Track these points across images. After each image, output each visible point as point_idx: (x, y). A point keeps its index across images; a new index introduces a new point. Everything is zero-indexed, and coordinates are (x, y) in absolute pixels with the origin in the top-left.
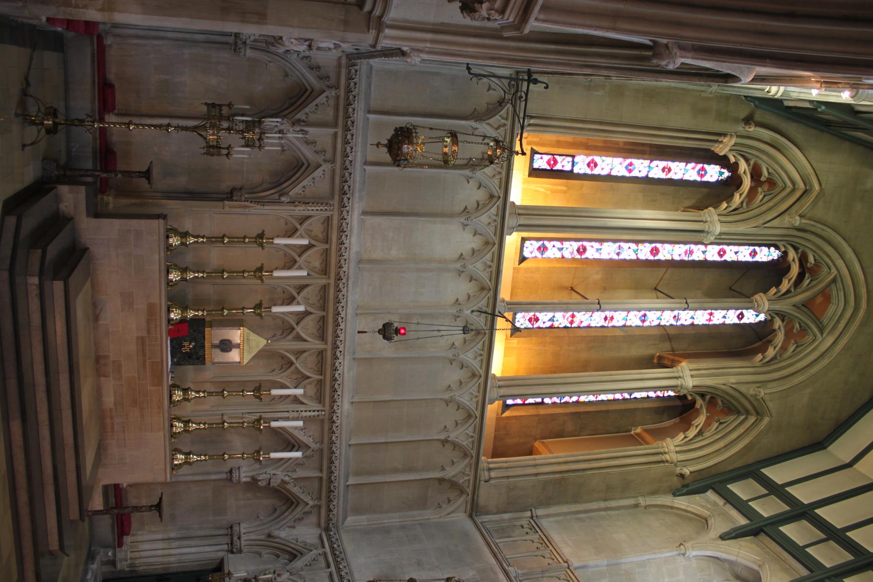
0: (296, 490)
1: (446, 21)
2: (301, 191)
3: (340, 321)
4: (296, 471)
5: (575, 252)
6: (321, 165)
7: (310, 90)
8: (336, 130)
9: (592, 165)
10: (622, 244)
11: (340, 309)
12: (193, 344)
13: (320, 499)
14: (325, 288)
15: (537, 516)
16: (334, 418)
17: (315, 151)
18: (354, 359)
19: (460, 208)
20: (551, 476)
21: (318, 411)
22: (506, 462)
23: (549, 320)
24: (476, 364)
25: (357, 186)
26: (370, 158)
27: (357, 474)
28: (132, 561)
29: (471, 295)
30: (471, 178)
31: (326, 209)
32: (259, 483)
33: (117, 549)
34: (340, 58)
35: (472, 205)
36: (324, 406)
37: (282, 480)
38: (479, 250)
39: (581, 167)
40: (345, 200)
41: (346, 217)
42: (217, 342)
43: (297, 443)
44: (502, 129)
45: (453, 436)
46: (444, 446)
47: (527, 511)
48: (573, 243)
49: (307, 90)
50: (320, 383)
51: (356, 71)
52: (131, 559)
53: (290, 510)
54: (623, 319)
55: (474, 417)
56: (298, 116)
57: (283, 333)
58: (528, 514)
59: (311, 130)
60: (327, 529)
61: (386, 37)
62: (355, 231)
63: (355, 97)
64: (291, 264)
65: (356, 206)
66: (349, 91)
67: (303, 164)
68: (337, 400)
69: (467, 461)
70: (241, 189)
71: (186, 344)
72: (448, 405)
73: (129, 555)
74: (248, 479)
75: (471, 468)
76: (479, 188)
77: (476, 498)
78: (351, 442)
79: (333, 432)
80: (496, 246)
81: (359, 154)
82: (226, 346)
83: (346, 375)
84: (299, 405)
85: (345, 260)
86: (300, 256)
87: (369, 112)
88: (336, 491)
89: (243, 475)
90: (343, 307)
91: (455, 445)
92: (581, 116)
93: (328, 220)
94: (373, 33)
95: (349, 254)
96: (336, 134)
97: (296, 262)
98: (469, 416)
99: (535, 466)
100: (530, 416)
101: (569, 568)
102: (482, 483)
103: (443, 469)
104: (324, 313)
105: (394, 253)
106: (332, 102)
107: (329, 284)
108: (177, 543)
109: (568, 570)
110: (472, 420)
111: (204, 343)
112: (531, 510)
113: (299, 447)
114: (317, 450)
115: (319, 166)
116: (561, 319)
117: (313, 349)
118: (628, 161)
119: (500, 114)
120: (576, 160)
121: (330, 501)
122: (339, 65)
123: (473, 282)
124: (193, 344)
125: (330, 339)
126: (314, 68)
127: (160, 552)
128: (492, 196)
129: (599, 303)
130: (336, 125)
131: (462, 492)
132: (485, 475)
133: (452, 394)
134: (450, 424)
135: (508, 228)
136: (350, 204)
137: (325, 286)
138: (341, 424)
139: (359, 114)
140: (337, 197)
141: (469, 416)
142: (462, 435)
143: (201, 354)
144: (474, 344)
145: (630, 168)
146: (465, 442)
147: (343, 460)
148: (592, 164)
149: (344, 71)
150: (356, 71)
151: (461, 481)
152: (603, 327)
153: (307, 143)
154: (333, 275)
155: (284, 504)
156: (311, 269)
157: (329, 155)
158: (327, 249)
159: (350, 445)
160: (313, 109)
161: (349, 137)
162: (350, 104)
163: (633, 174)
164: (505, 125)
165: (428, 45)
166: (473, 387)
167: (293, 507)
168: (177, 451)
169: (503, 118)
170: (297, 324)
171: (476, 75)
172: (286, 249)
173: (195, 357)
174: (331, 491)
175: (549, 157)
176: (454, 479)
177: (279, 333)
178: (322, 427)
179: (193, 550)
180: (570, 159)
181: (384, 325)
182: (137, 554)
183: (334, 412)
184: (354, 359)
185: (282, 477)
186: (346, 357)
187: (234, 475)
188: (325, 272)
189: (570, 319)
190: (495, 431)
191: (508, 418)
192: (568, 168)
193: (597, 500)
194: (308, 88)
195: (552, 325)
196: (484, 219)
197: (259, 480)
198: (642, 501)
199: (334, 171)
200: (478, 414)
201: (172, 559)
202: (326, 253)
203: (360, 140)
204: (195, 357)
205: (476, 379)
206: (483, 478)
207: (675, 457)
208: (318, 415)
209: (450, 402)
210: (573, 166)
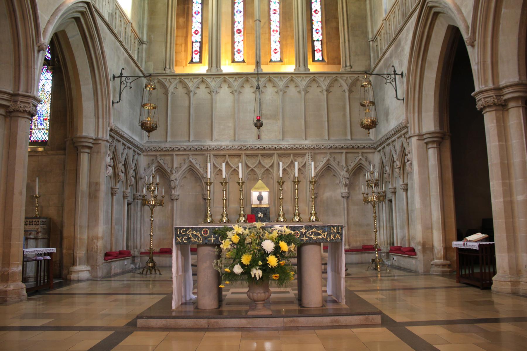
0: (353, 165)
1: (93, 114)
2: (202, 169)
3: (262, 147)
4: (342, 165)
5: (240, 34)
6: (190, 161)
7: (158, 167)
8: (174, 155)
9: (196, 32)
10: (235, 11)
11: (256, 148)
12: (259, 212)
13: (358, 153)
14: (247, 155)
15: (372, 38)
16: (312, 147)
17: (184, 163)
18: (283, 140)
19: (209, 96)
20: (350, 33)
21: (309, 156)
22: (343, 58)
23: (276, 43)
25: (199, 144)
26: (187, 139)
27: (346, 135)
28: (388, 244)
29: (250, 86)
30: (194, 92)
31: (210, 157)
32: (347, 183)
33: (381, 251)
34: (144, 155)
35: (207, 90)
36: (307, 153)
37: (346, 172)
38: (229, 85)
39: (198, 38)
40: (204, 149)
41: (212, 148)
42: (258, 202)
43: (327, 165)
44: (171, 80)
45: (325, 88)
46: (331, 92)
47: (369, 44)
48: (235, 37)
49: (158, 169)
50: (295, 155)
51: (148, 148)
52: (387, 245)
53: (365, 168)
54: (275, 4)
55: (314, 78)
56: (169, 171)
57: (270, 174)
58: (371, 43)
59: (175, 165)
60: (375, 148)
61: (103, 137)
62: (219, 143)
63: (159, 148)
64: (236, 171)
65: (209, 143)
66: (157, 151)
67: (190, 168)
68: (303, 147)
69: (340, 79)
70: (203, 195)
71: (259, 215)
72: (308, 92)
73: (386, 246)
74: (346, 188)
75: (343, 77)
76: (199, 88)
77: (359, 72)
78: (327, 138)
79: (320, 148)
80: (225, 77)
81: (184, 144)
82: (260, 198)
83: (290, 143)
84: (307, 165)
85: (233, 147)
86: (232, 168)
87: (189, 141)
88: (353, 145)
89: (344, 191)
90: (255, 146)
91: (330, 86)
92: (164, 44)
93: (215, 156)
94: (100, 142)
95: (230, 145)
96: (176, 155)
97: (235, 170)
99: (345, 42)
100: (327, 47)
101: (385, 19)
102: (352, 70)
103: (344, 91)
104: (260, 155)
105: (231, 125)
106: (163, 158)
107: (245, 154)
108: (381, 223)
109: (386, 19)
110: (316, 79)
111: (259, 208)
112: (369, 42)
113: (329, 164)
114: (331, 155)
115: (190, 161)
116: (275, 37)
117: (277, 160)
118: (194, 14)
119: (164, 82)
120: (194, 41)
121: (358, 147)
122: (147, 155)
123: (244, 86)
124: (259, 212)
125: (272, 152)
126: (149, 166)
127: (385, 231)
128: (203, 81)
129: (256, 21)
130: (172, 155)
131: (357, 80)
132: (348, 68)
133: (302, 90)
134: (319, 90)
135: (218, 72)
136: (207, 146)
137: (246, 155)
138: (316, 144)
139: (167, 145)
140: (204, 153)
141: (314, 80)
142: (324, 83)
143: (264, 209)
144: (275, 82)
145: (197, 13)
146: (327, 82)
147: (336, 142)
148: (196, 32)
149: (149, 153)
150: (148, 148)
151: (350, 81)
152: (279, 14)
153: (180, 167)
154: (240, 152)
155: (363, 171)
156: (239, 162)
157: (186, 157)
158: (229, 156)
159: (329, 139)
160: (166, 165)
161: (176, 149)
162: (162, 150)
163: (200, 11)
164: (169, 79)
165: (105, 120)
166: (298, 80)
167: (362, 166)
169: (166, 81)
170: (265, 167)
171: (120, 99)
172: (229, 174)
173: (265, 212)
174: (353, 147)
175: (193, 54)
176: (349, 85)
177: (271, 176)
178: (318, 153)
179: (384, 215)
180: (194, 44)
181: (256, 127)
182: (386, 242)
183: (309, 148)
184: (283, 140)
185: (345, 172)
186: (281, 144)
187: (344, 195)
188: (239, 156)
189: (275, 32)
190: (335, 64)
191: (328, 58)
192: (198, 44)
193: (365, 6)
194: (157, 168)
195: (278, 41)
197: (345, 183)
199: (192, 155)
200: (312, 76)
201: (388, 225)
202: (230, 156)
203: (178, 144)
204: (265, 212)
205: (294, 79)
206: (349, 70)
208: (311, 155)
209: (306, 90)
210: (197, 42)
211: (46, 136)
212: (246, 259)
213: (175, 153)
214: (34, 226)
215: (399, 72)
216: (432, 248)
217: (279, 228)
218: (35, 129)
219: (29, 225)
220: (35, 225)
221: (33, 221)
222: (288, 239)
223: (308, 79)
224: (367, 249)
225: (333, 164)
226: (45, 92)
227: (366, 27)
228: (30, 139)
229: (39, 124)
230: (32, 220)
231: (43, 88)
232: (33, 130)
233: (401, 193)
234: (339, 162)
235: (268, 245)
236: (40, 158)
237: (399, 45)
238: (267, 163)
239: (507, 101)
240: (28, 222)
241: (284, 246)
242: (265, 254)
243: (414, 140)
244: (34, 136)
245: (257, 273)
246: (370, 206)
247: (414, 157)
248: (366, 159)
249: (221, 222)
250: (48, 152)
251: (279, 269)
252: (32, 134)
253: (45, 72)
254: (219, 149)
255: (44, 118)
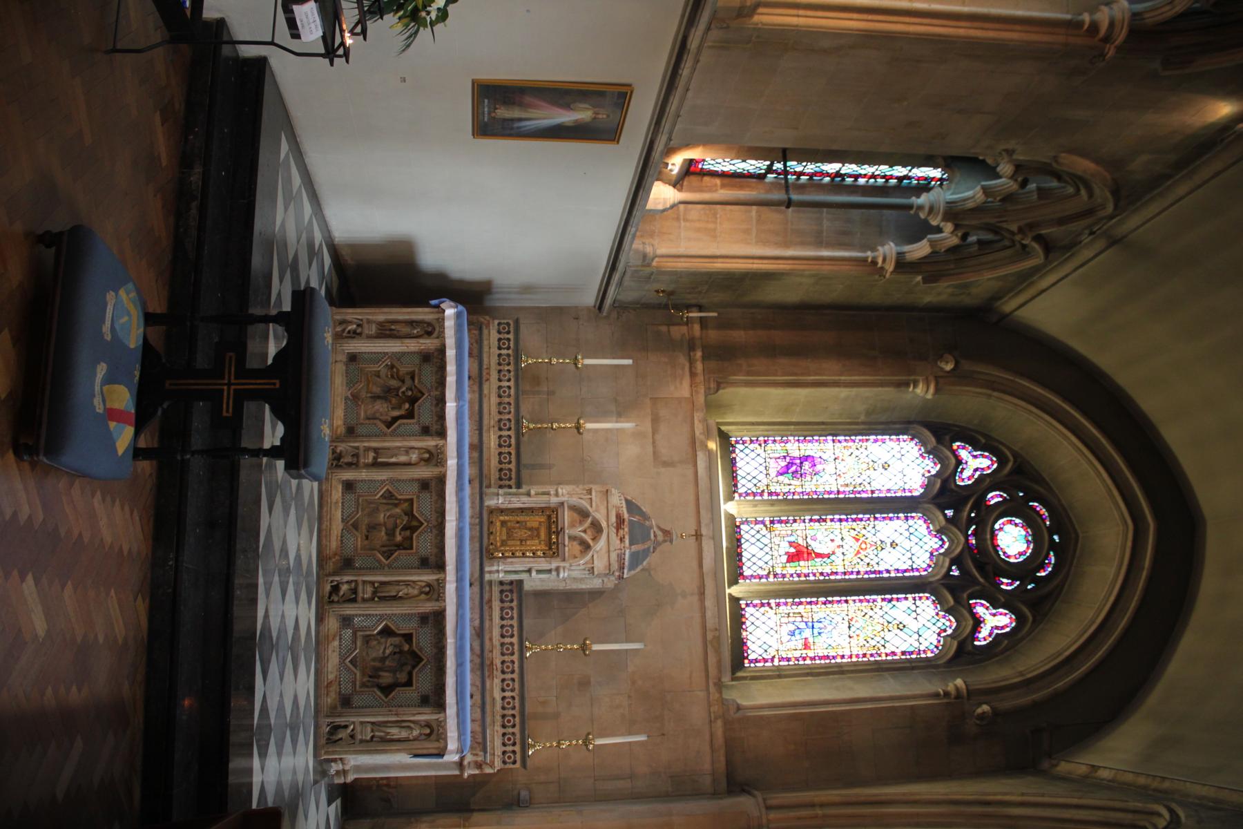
211: (760, 651)
214: (499, 750)
218: (779, 616)
219: (504, 735)
220: (504, 753)
221: (514, 744)
226: (882, 634)
228: (747, 605)
229: (792, 627)
230: (518, 741)
231: (896, 626)
232: (774, 611)
236: (702, 694)
240: (511, 730)
244: (758, 614)
250: (719, 723)
252: (763, 609)
253: (939, 624)
255: (811, 640)
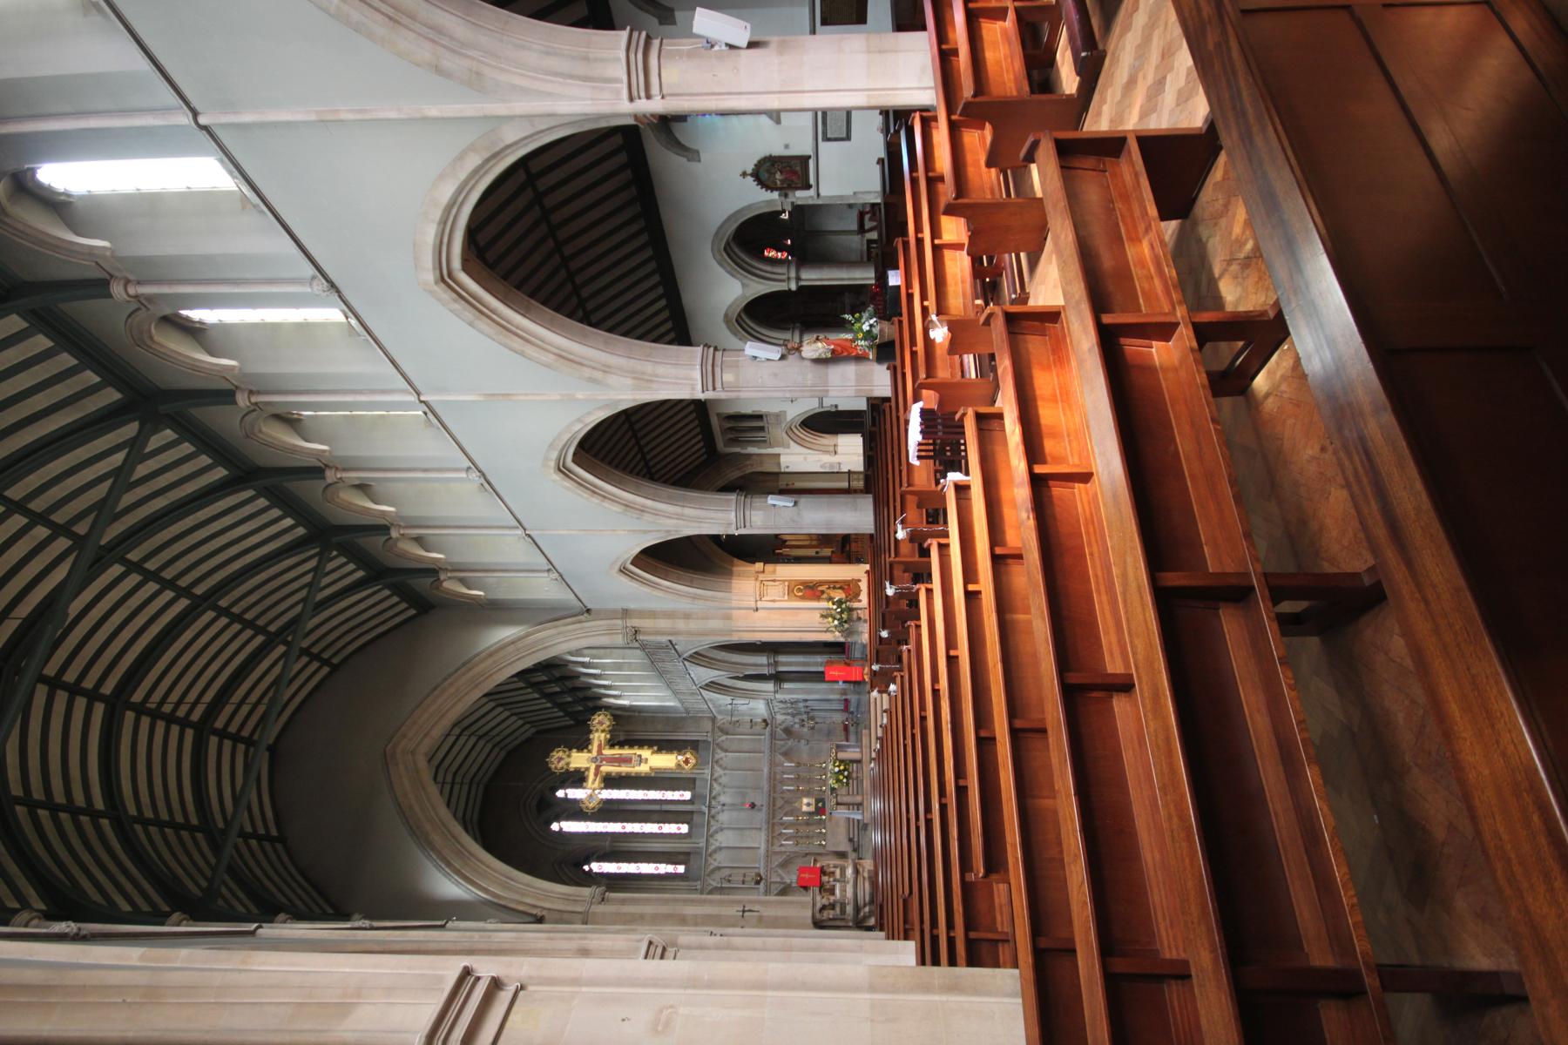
0: (784, 736)
14: (773, 818)
24: (715, 785)
45: (723, 754)
56: (782, 886)
59: (779, 880)
60: (773, 718)
62: (763, 841)
78: (762, 754)
82: (808, 805)
93: (772, 845)
98: (717, 762)
115: (777, 866)
130: (771, 883)
146: (719, 751)
166: (716, 775)
168: (824, 768)
188: (773, 824)
196: (713, 847)
198: (637, 714)
202: (773, 832)
207: (621, 733)
212: (841, 777)
213: (769, 880)
215: (730, 702)
216: (844, 689)
217: (831, 767)
222: (835, 763)
223: (715, 766)
224: (846, 728)
225: (784, 749)
227: (676, 718)
233: (808, 704)
234: (783, 746)
235: (837, 769)
237: (711, 700)
238: (779, 803)
239: (775, 661)
241: (837, 764)
242: (840, 771)
243: (777, 696)
245: (846, 773)
246: (816, 726)
247: (787, 697)
248: (780, 725)
249: (825, 834)
251: (845, 766)
254: (768, 841)
